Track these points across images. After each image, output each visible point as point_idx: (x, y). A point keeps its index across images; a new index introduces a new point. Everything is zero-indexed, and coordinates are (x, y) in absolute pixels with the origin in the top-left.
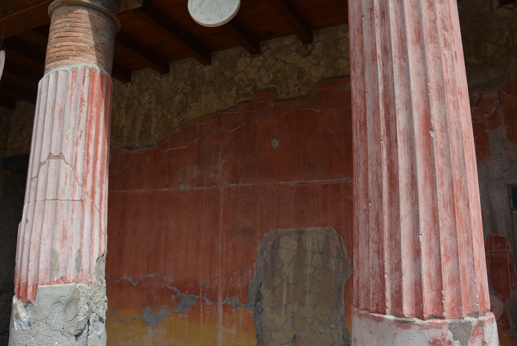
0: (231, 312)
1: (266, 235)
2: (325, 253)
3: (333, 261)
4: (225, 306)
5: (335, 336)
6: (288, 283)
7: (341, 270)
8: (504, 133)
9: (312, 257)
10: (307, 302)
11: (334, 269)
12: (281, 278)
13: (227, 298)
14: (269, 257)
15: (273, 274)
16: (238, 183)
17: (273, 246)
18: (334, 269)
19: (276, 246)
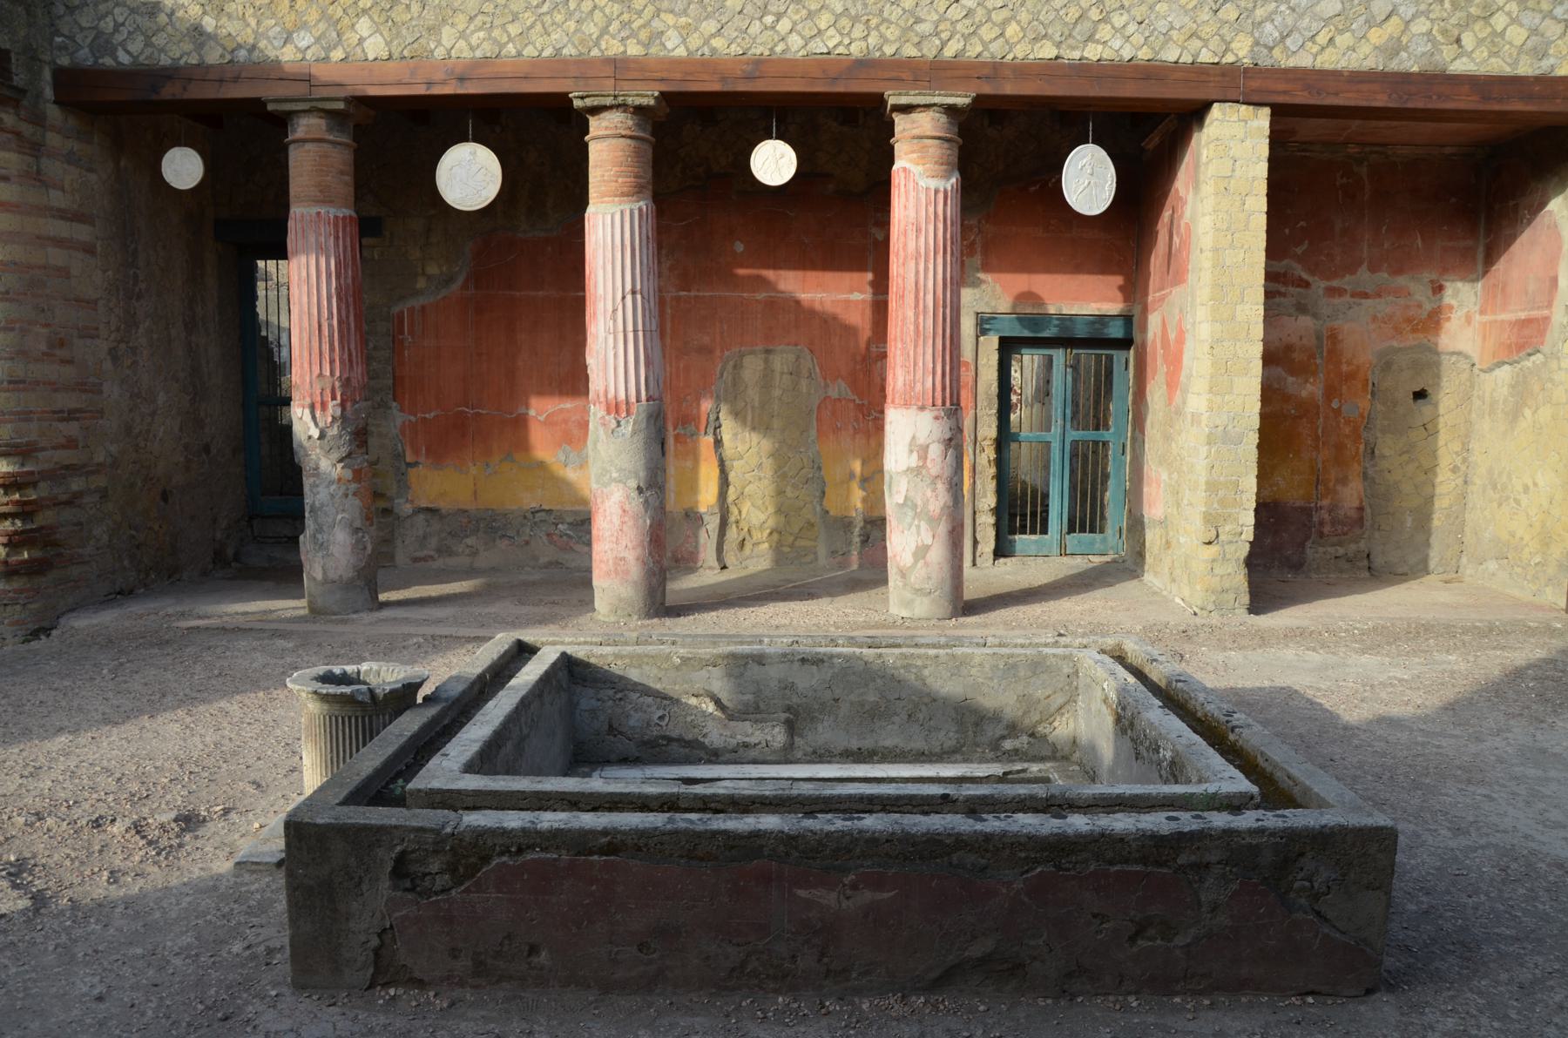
0: (686, 442)
1: (727, 353)
2: (795, 373)
3: (804, 383)
4: (677, 437)
5: (805, 460)
6: (753, 407)
7: (812, 391)
8: (979, 262)
9: (781, 379)
10: (775, 426)
11: (804, 391)
12: (745, 402)
13: (680, 426)
14: (730, 378)
15: (736, 398)
16: (689, 291)
17: (735, 367)
18: (804, 391)
19: (737, 367)
